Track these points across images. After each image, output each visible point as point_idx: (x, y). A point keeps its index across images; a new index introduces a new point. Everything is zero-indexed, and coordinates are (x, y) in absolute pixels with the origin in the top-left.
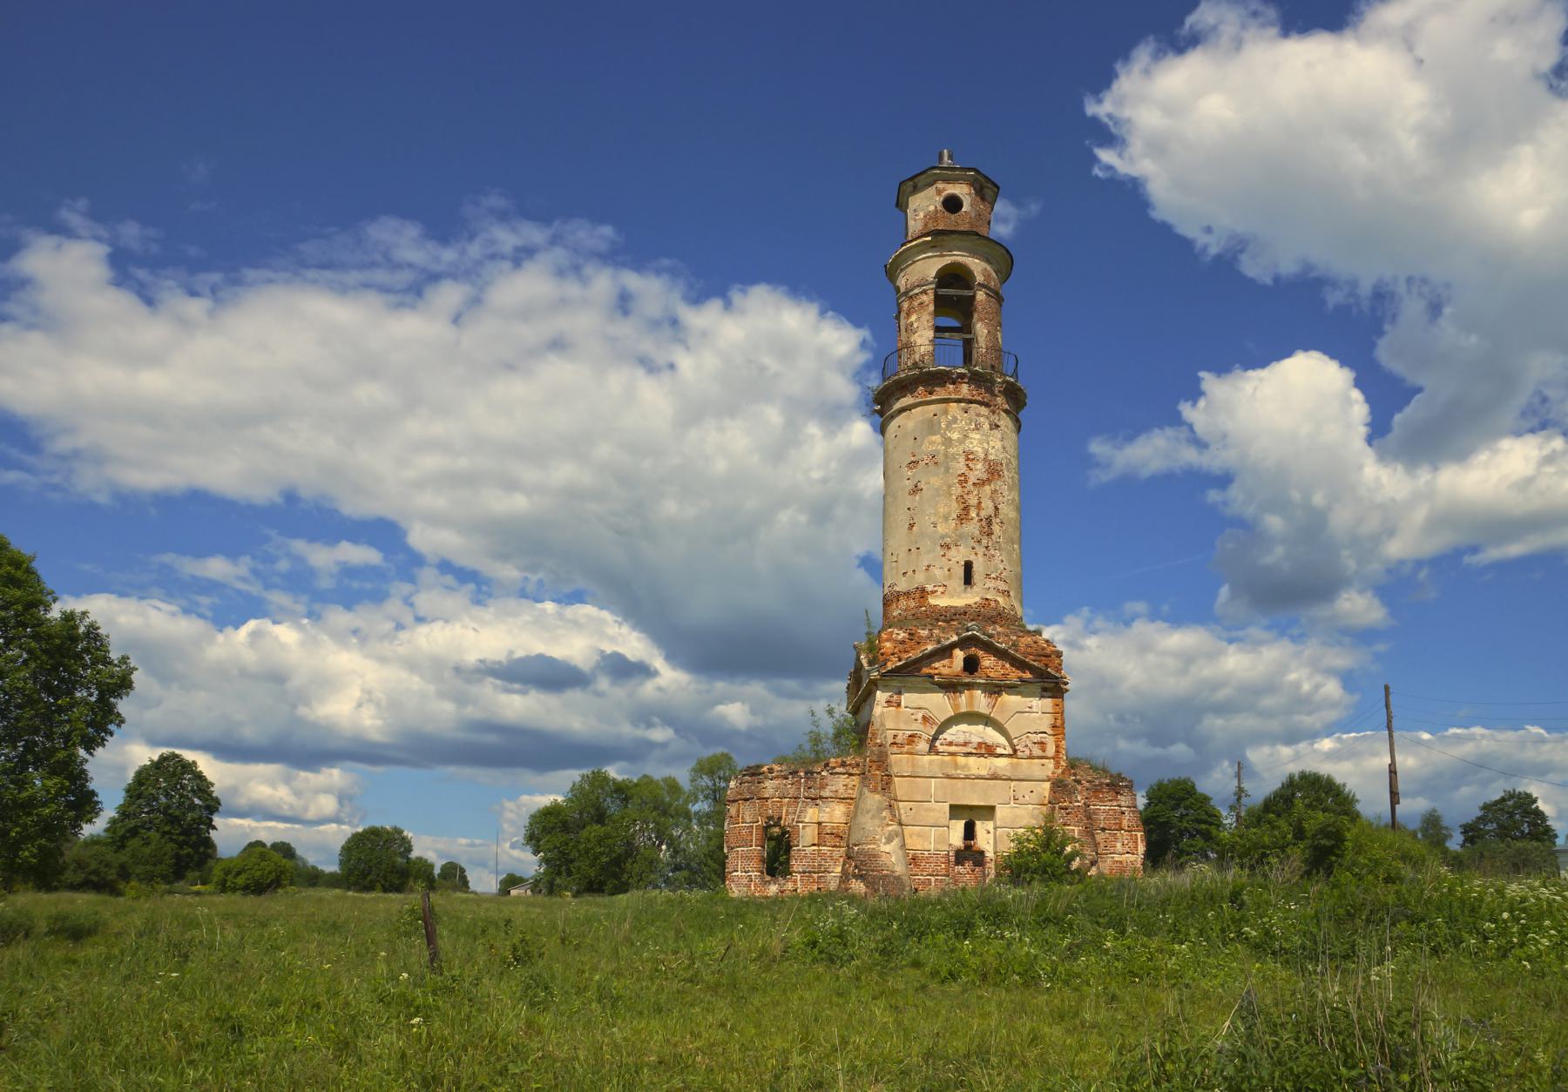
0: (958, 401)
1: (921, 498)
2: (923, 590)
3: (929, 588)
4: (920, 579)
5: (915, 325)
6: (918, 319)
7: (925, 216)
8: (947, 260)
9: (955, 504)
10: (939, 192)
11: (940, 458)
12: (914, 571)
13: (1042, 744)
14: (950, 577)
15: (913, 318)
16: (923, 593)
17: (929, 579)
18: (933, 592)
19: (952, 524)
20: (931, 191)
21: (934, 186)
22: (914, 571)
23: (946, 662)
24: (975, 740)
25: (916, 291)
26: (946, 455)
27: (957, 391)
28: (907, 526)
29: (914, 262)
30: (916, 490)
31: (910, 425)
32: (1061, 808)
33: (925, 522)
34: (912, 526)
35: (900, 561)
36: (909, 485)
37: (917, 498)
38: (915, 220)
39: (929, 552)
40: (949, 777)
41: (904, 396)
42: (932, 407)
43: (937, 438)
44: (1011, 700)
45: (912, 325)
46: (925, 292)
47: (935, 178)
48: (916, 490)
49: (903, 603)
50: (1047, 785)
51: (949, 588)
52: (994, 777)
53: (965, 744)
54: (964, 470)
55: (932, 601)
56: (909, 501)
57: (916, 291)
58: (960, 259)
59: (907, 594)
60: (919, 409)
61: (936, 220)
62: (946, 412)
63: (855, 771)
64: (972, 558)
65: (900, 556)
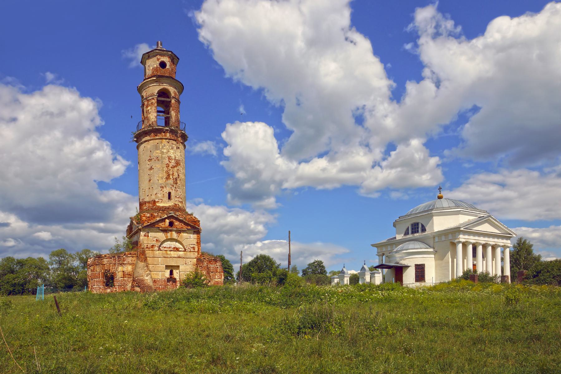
1: (153, 171)
2: (154, 201)
3: (157, 200)
4: (153, 197)
5: (150, 111)
7: (153, 69)
9: (165, 174)
11: (160, 158)
14: (164, 197)
15: (149, 108)
16: (154, 202)
17: (156, 198)
18: (158, 202)
21: (156, 57)
22: (151, 195)
23: (163, 223)
25: (150, 98)
26: (162, 157)
27: (165, 136)
29: (149, 87)
30: (151, 169)
31: (149, 147)
33: (155, 179)
34: (150, 180)
36: (149, 167)
37: (152, 171)
38: (149, 70)
41: (146, 136)
42: (157, 141)
43: (158, 151)
45: (148, 111)
48: (151, 169)
49: (147, 205)
51: (164, 200)
55: (158, 204)
56: (149, 172)
57: (150, 98)
58: (166, 87)
59: (149, 202)
60: (152, 141)
61: (157, 71)
62: (162, 143)
64: (171, 191)
65: (146, 190)
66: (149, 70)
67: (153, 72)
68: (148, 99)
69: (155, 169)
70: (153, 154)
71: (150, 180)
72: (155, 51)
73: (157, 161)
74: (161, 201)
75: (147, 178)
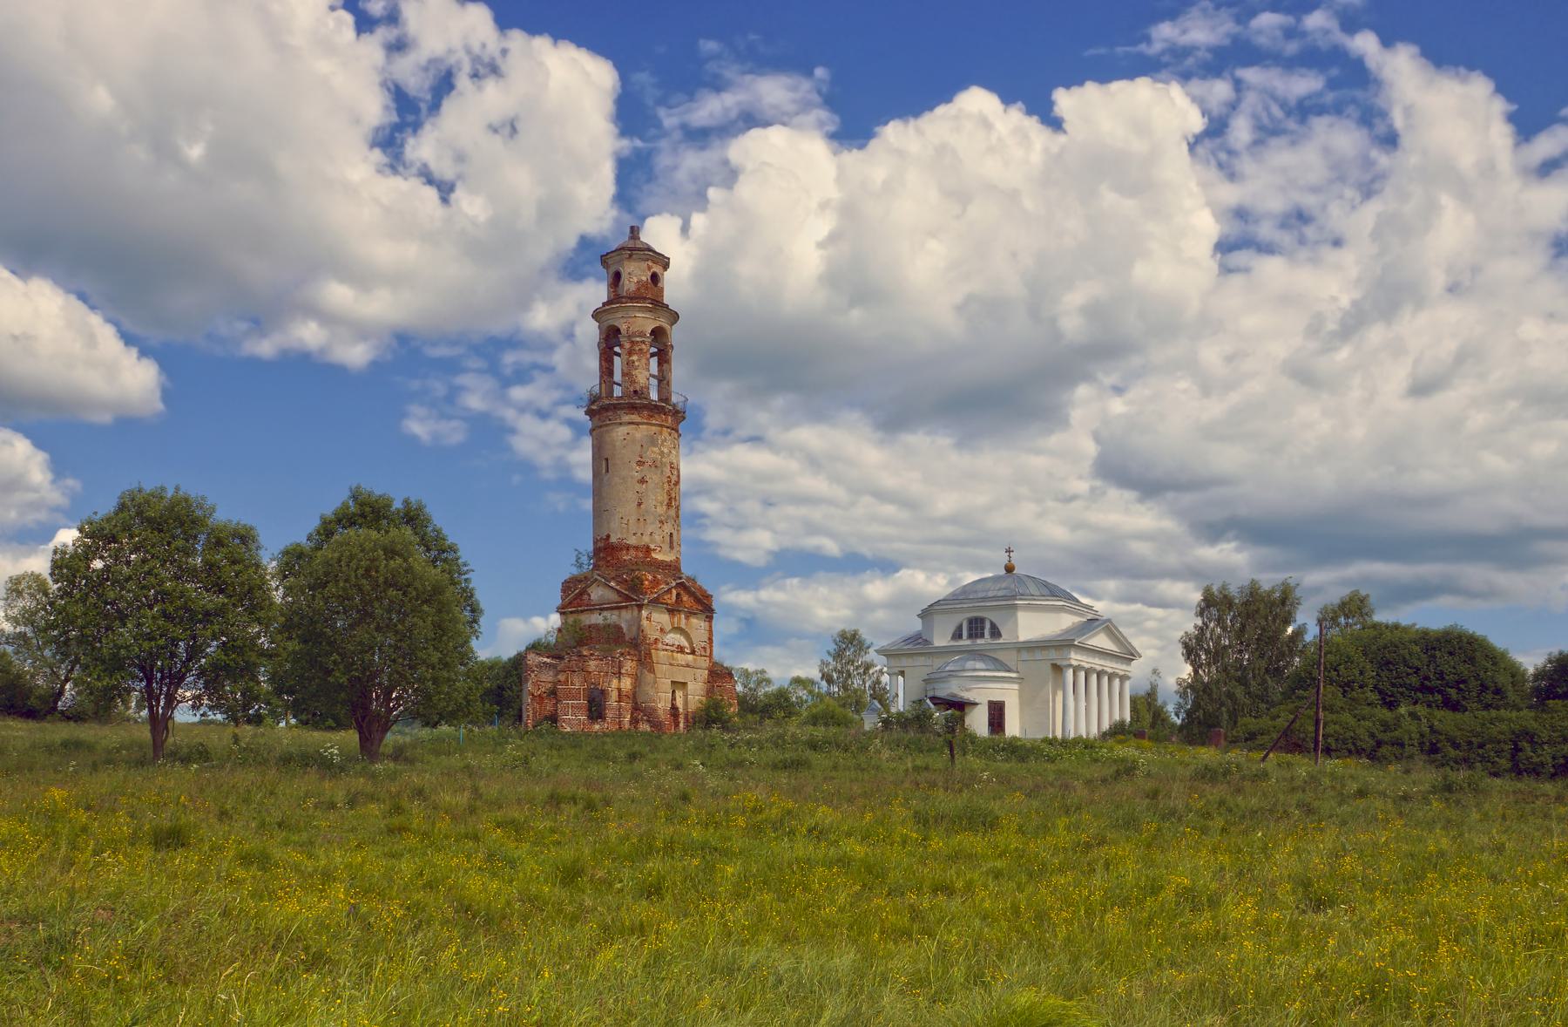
0: (668, 428)
1: (646, 486)
2: (648, 547)
3: (652, 547)
4: (646, 539)
5: (637, 364)
6: (639, 360)
8: (657, 324)
10: (649, 268)
13: (704, 648)
14: (663, 542)
15: (635, 358)
16: (648, 550)
17: (652, 541)
18: (654, 550)
19: (665, 508)
20: (644, 265)
23: (669, 596)
24: (677, 643)
25: (638, 339)
27: (666, 421)
30: (642, 481)
31: (638, 435)
32: (717, 686)
34: (640, 504)
35: (630, 525)
36: (638, 476)
37: (644, 486)
39: (653, 523)
40: (671, 664)
42: (654, 428)
43: (656, 449)
44: (694, 621)
45: (634, 362)
46: (643, 342)
47: (648, 257)
48: (642, 481)
49: (632, 552)
50: (707, 672)
51: (664, 549)
52: (688, 666)
53: (673, 645)
54: (669, 474)
55: (654, 555)
56: (638, 487)
57: (638, 339)
58: (663, 324)
59: (636, 548)
60: (645, 426)
61: (647, 288)
62: (661, 433)
63: (635, 658)
67: (638, 289)
68: (634, 339)
69: (651, 485)
71: (640, 504)
72: (646, 252)
73: (653, 468)
74: (659, 549)
75: (631, 496)
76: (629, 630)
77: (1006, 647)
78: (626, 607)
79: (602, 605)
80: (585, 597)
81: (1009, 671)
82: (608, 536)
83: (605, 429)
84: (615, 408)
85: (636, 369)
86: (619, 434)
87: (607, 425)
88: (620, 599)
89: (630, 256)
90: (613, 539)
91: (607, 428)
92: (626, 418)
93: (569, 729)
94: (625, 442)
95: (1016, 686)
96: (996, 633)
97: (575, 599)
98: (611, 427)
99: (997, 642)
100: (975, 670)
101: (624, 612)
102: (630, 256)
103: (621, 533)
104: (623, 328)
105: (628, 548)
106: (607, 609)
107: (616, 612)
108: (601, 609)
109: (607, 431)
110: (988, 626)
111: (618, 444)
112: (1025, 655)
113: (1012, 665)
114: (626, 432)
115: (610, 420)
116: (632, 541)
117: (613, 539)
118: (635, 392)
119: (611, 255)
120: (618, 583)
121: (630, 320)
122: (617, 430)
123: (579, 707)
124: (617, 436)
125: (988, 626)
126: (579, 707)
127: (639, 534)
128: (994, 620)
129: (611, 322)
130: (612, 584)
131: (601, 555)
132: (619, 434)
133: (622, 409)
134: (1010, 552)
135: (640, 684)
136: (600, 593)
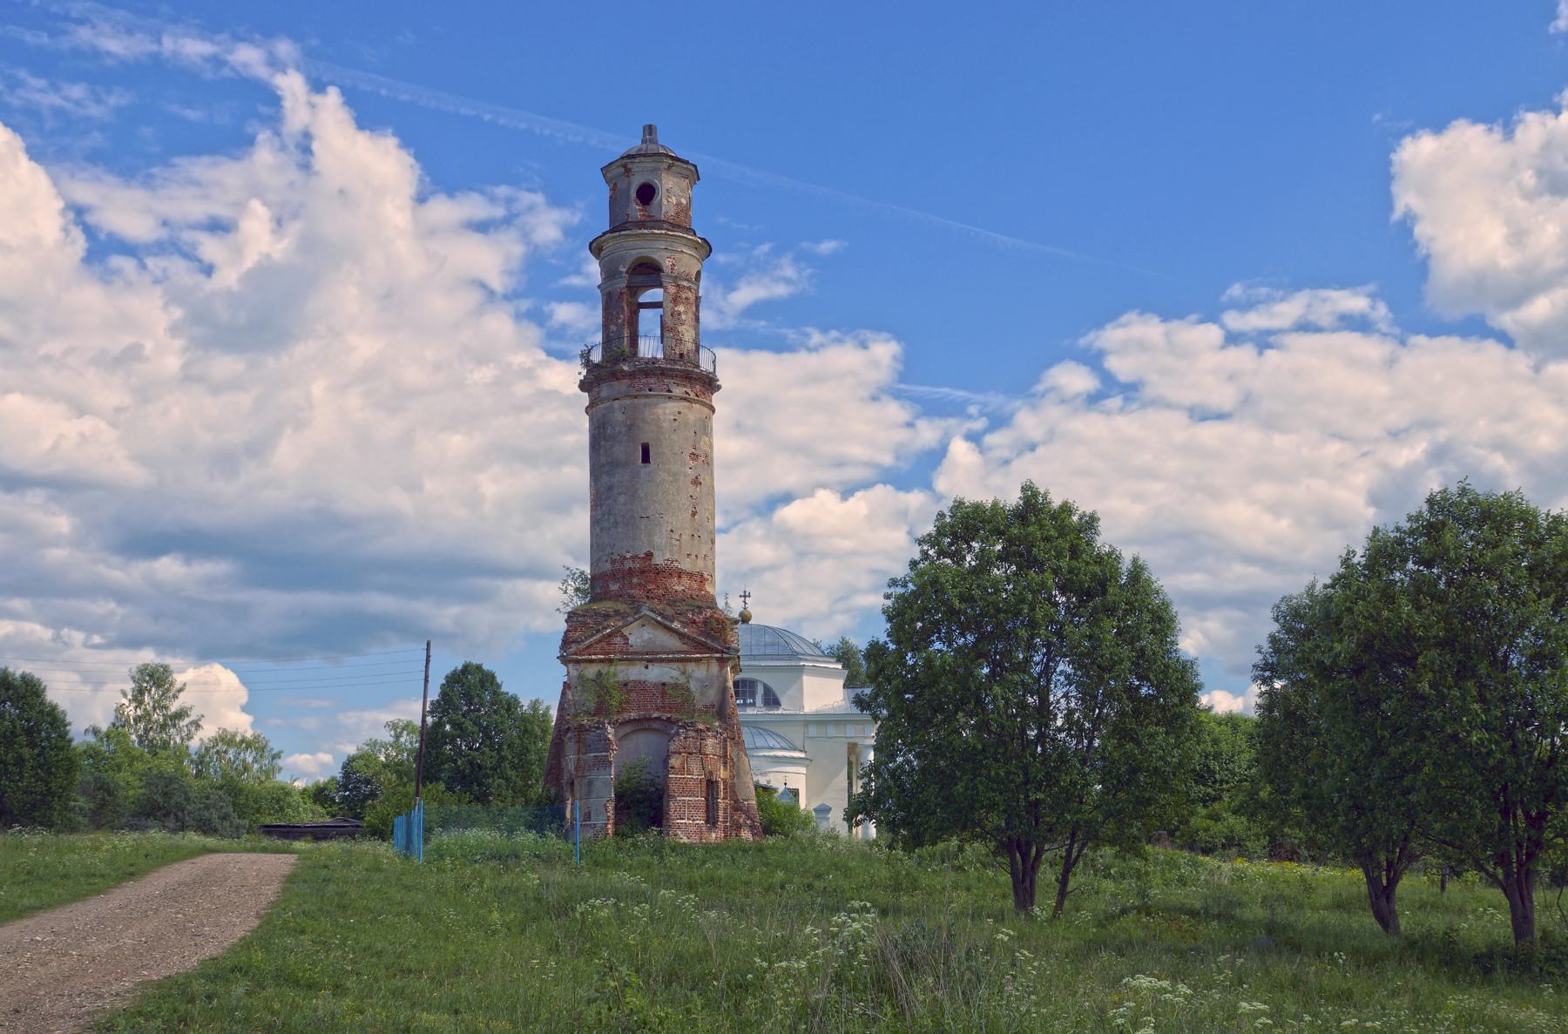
5: (683, 317)
12: (696, 556)
15: (681, 308)
22: (696, 556)
25: (685, 283)
28: (690, 512)
34: (694, 514)
37: (698, 489)
38: (668, 202)
45: (679, 314)
49: (685, 581)
56: (691, 489)
57: (685, 283)
59: (691, 575)
65: (684, 537)
66: (668, 202)
68: (680, 283)
70: (699, 443)
71: (694, 514)
76: (702, 694)
77: (789, 720)
78: (698, 660)
79: (658, 653)
80: (618, 640)
81: (795, 749)
82: (649, 555)
83: (643, 401)
84: (663, 374)
85: (682, 324)
86: (667, 411)
87: (647, 396)
88: (685, 647)
89: (670, 167)
90: (659, 559)
91: (647, 400)
92: (678, 391)
93: (685, 840)
94: (676, 423)
95: (803, 770)
96: (772, 700)
97: (599, 641)
98: (655, 400)
99: (776, 712)
100: (772, 748)
101: (691, 667)
102: (670, 167)
103: (671, 552)
104: (667, 264)
105: (680, 574)
106: (661, 661)
107: (680, 665)
108: (650, 661)
109: (646, 405)
110: (760, 691)
111: (665, 425)
112: (813, 731)
113: (798, 744)
114: (677, 410)
115: (650, 390)
116: (686, 565)
117: (659, 559)
118: (681, 355)
119: (642, 159)
120: (684, 624)
121: (677, 256)
122: (664, 405)
123: (696, 808)
124: (664, 414)
125: (760, 691)
126: (696, 808)
127: (694, 557)
128: (765, 681)
129: (645, 252)
130: (676, 625)
131: (635, 580)
132: (667, 411)
133: (672, 377)
134: (745, 596)
135: (738, 775)
136: (646, 636)
